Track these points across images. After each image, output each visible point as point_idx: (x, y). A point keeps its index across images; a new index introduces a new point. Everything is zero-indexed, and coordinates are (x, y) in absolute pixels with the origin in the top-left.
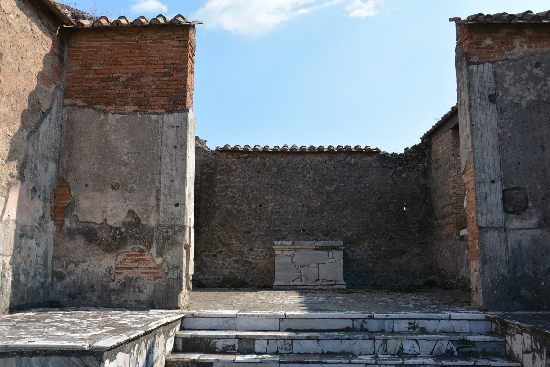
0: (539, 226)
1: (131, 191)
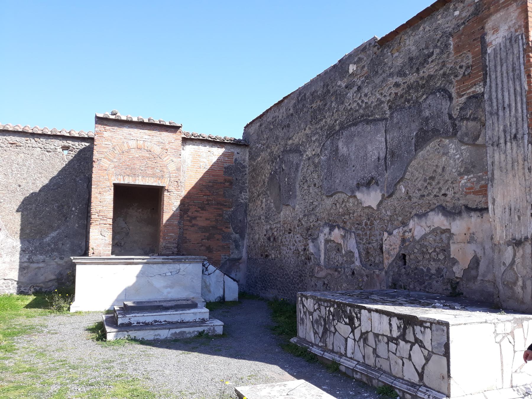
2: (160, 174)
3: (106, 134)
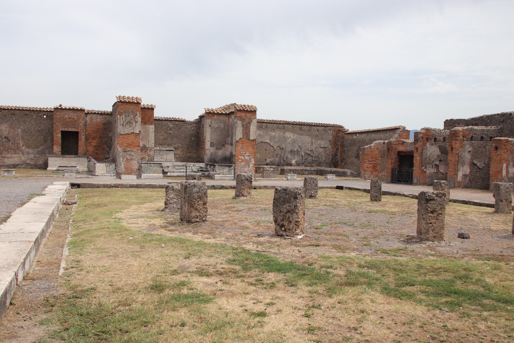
2: (77, 127)
3: (58, 113)
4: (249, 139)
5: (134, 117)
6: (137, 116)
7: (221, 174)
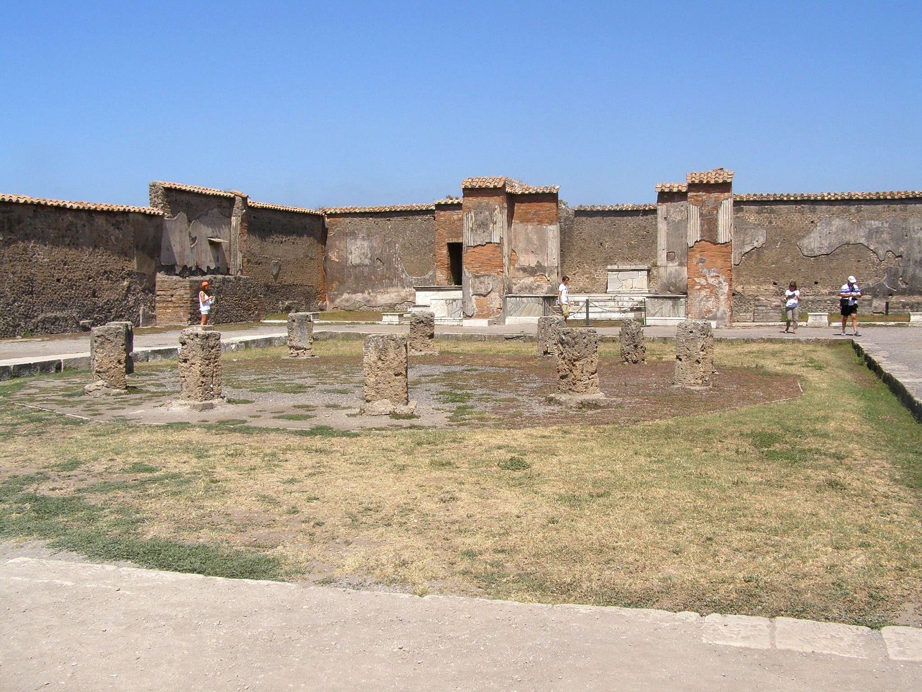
0: (679, 265)
1: (538, 254)
4: (715, 243)
5: (491, 214)
6: (496, 212)
7: (658, 314)
